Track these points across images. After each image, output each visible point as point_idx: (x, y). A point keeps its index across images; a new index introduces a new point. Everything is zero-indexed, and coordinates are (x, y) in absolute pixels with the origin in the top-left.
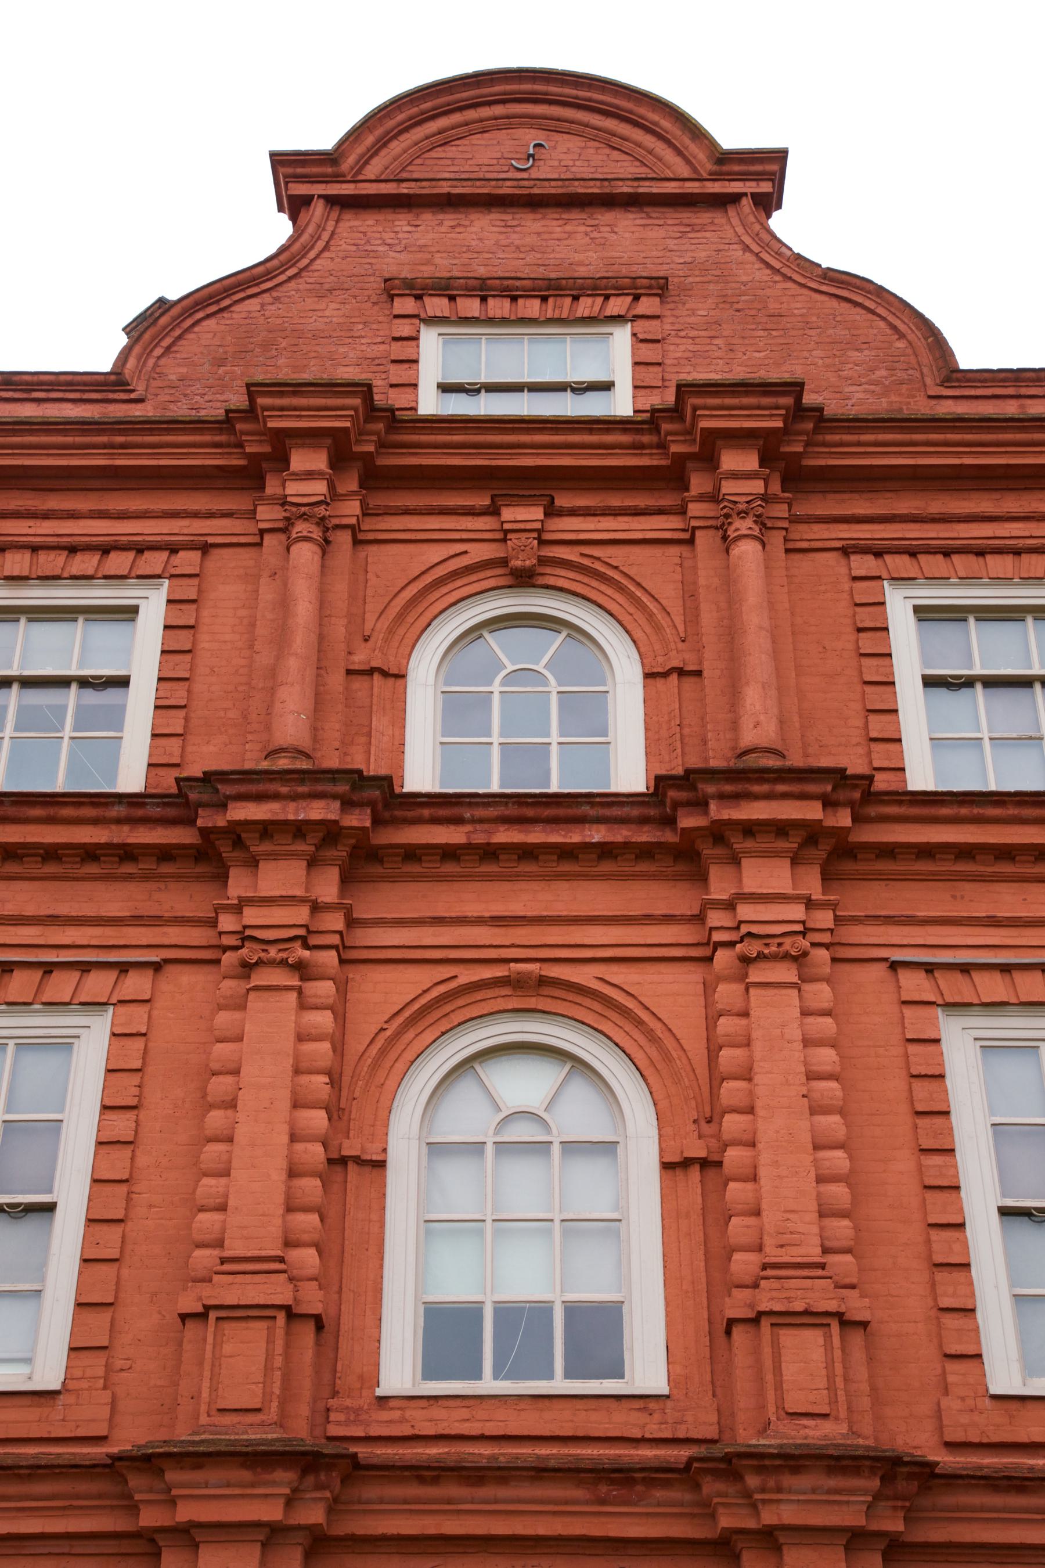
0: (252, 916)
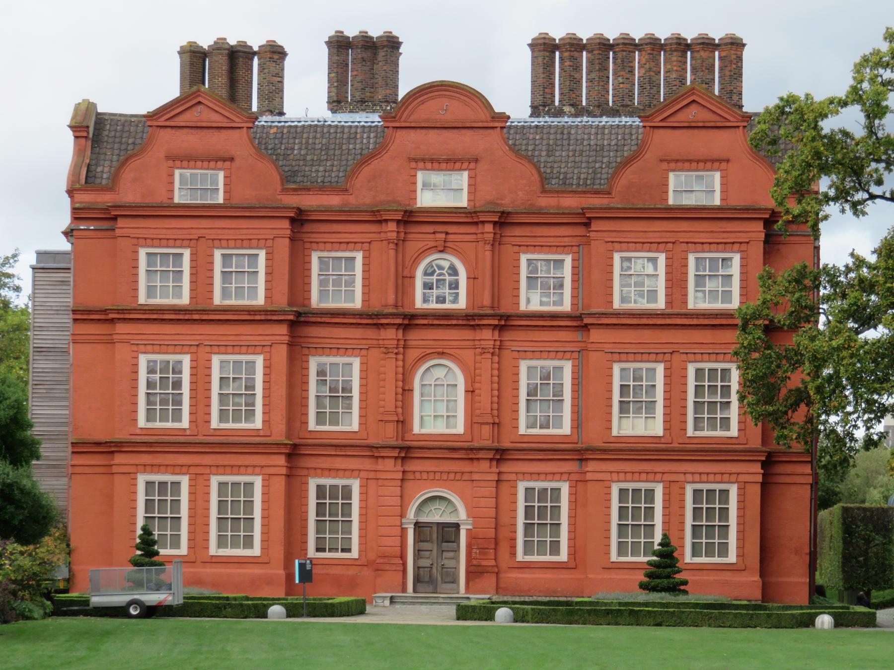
0: (386, 342)
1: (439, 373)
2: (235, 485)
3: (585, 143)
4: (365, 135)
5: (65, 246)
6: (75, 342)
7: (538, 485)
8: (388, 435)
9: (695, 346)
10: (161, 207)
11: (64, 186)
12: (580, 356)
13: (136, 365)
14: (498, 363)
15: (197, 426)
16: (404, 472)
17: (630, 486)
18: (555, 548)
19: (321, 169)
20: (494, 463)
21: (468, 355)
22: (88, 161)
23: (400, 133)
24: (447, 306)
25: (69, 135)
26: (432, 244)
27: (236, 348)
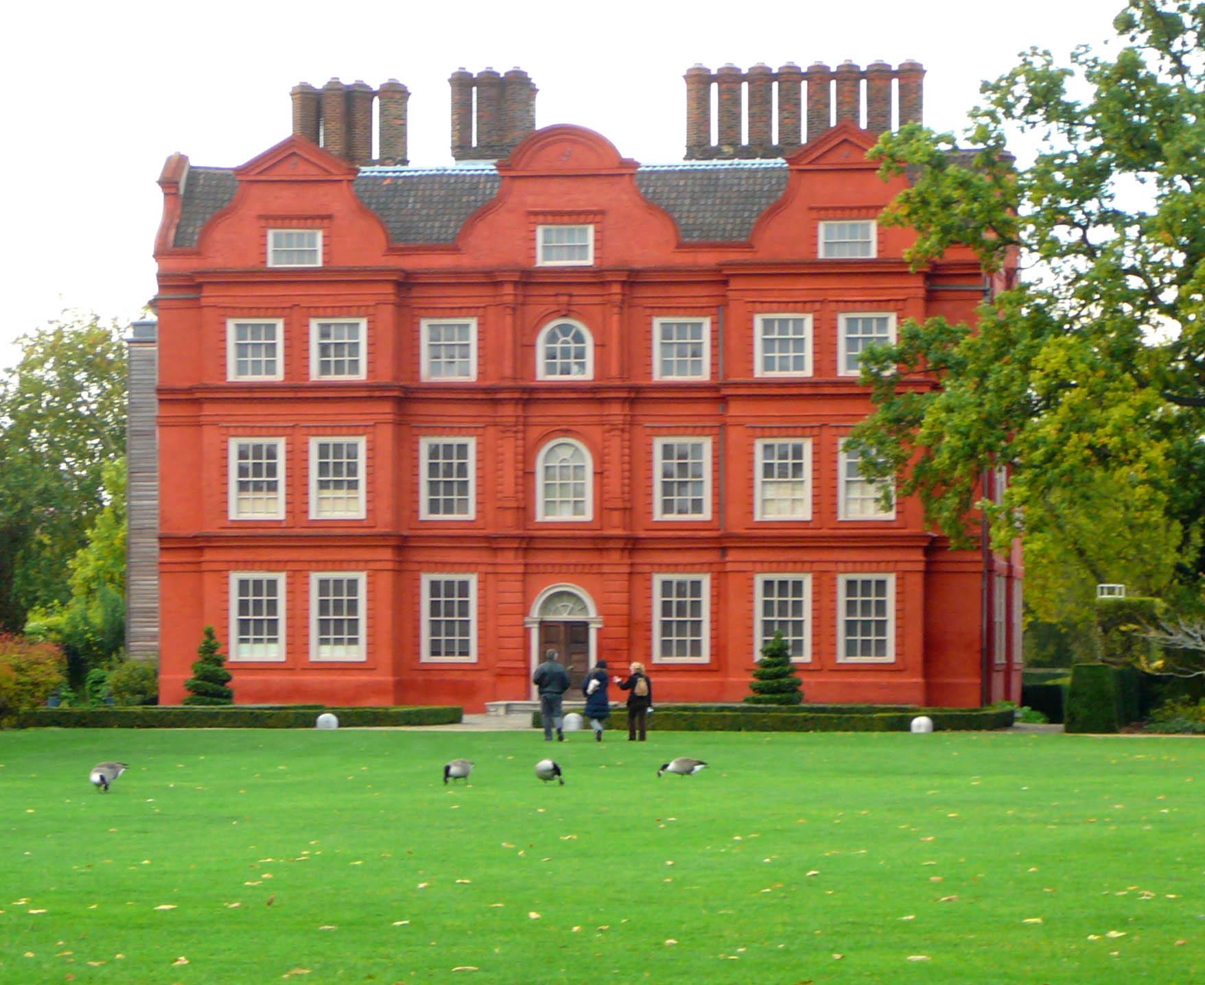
1: (565, 453)
2: (338, 582)
3: (735, 189)
4: (489, 185)
5: (152, 317)
6: (162, 425)
7: (675, 577)
8: (507, 524)
9: (846, 418)
10: (253, 273)
11: (151, 249)
12: (720, 432)
13: (226, 450)
14: (629, 440)
15: (294, 517)
16: (526, 565)
17: (776, 577)
18: (696, 649)
19: (437, 224)
20: (627, 552)
21: (596, 433)
22: (177, 221)
23: (518, 183)
25: (158, 196)
26: (555, 308)
27: (336, 430)
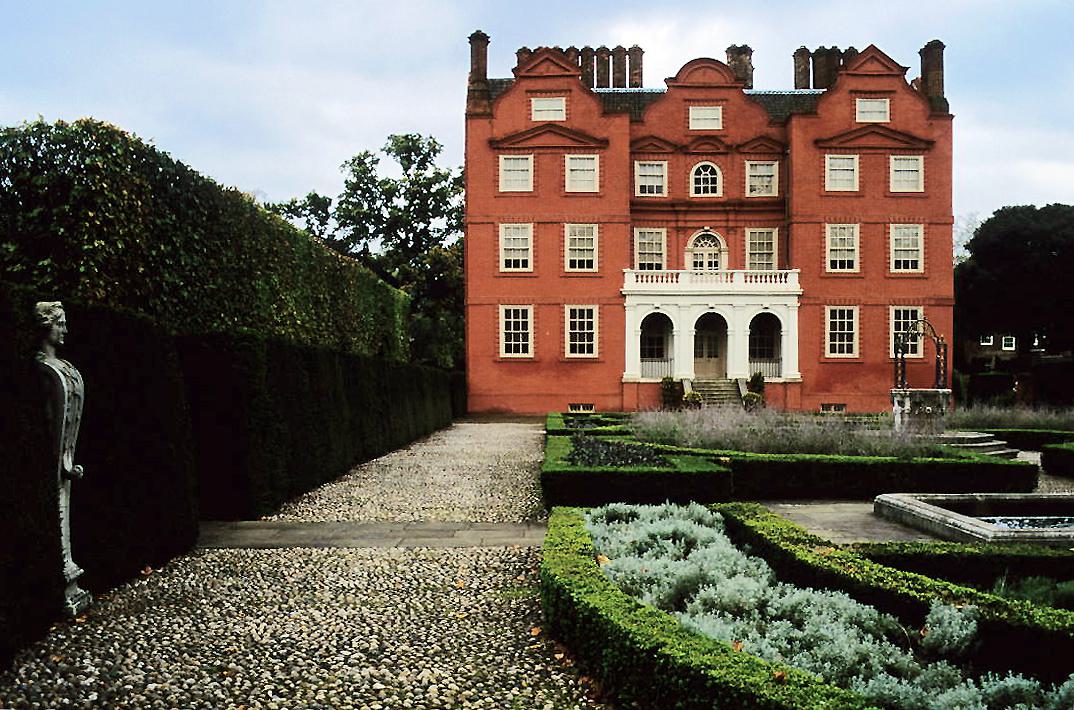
24: (710, 195)
